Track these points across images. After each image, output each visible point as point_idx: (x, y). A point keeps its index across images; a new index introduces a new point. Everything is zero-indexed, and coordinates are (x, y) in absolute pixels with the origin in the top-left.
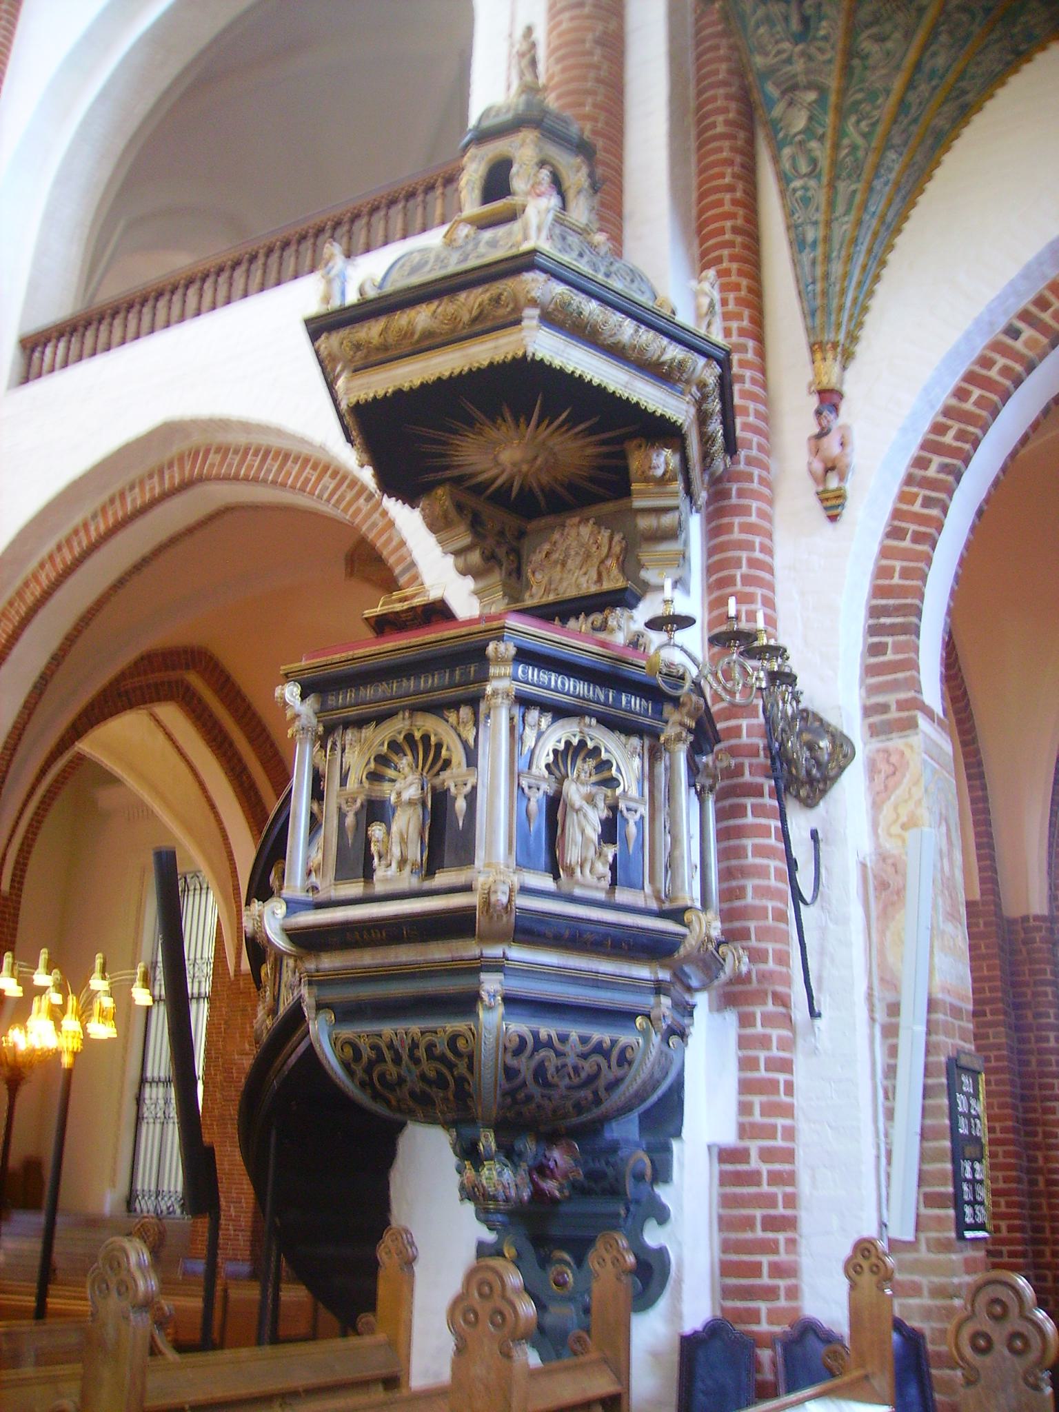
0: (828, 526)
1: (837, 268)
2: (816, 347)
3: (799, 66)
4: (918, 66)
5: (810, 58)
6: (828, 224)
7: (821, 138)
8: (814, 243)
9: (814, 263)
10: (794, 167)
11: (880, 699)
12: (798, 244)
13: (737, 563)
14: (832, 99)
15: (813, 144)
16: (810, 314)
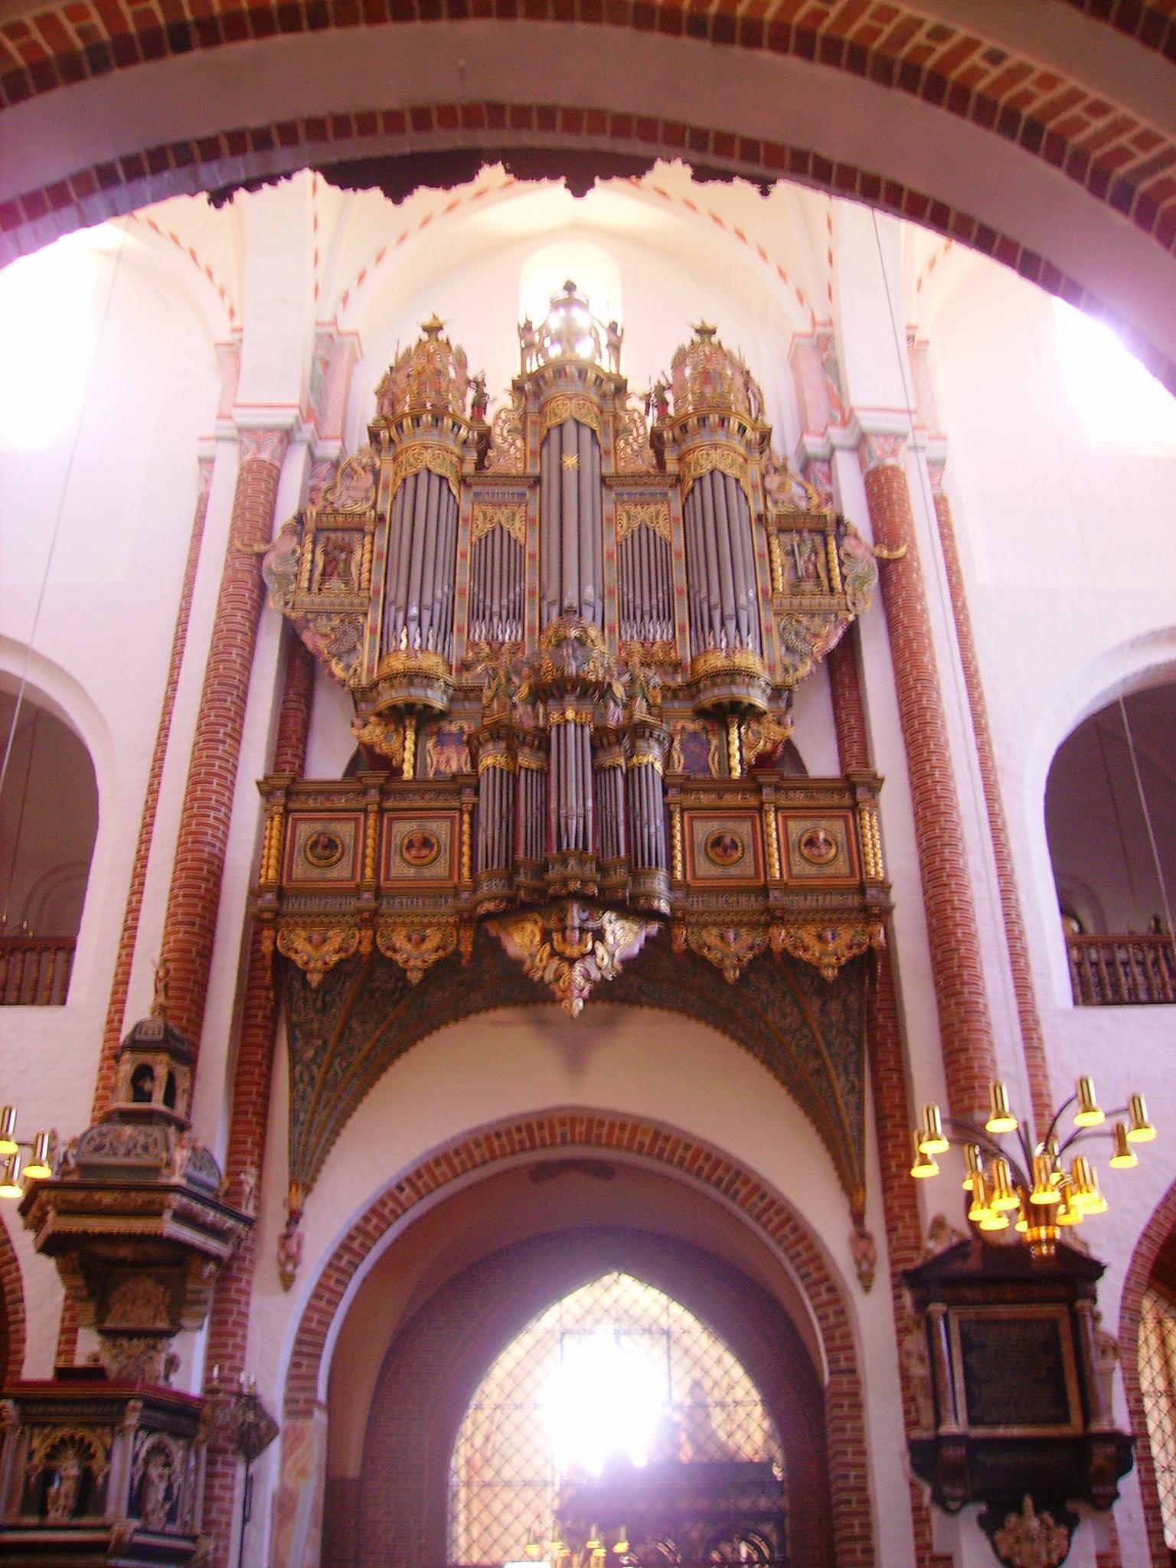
0: (283, 1293)
1: (313, 1139)
2: (293, 1183)
3: (316, 1025)
4: (378, 1041)
5: (322, 1022)
6: (313, 1114)
7: (320, 1066)
8: (303, 1123)
9: (300, 1135)
10: (301, 1077)
11: (295, 1395)
12: (294, 1120)
13: (230, 1312)
14: (330, 1047)
15: (315, 1069)
16: (293, 1163)
